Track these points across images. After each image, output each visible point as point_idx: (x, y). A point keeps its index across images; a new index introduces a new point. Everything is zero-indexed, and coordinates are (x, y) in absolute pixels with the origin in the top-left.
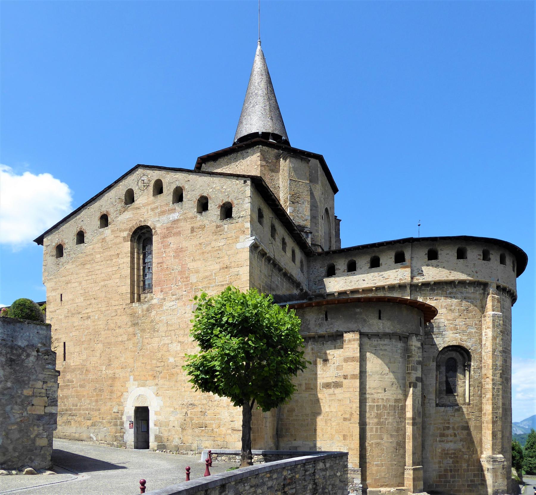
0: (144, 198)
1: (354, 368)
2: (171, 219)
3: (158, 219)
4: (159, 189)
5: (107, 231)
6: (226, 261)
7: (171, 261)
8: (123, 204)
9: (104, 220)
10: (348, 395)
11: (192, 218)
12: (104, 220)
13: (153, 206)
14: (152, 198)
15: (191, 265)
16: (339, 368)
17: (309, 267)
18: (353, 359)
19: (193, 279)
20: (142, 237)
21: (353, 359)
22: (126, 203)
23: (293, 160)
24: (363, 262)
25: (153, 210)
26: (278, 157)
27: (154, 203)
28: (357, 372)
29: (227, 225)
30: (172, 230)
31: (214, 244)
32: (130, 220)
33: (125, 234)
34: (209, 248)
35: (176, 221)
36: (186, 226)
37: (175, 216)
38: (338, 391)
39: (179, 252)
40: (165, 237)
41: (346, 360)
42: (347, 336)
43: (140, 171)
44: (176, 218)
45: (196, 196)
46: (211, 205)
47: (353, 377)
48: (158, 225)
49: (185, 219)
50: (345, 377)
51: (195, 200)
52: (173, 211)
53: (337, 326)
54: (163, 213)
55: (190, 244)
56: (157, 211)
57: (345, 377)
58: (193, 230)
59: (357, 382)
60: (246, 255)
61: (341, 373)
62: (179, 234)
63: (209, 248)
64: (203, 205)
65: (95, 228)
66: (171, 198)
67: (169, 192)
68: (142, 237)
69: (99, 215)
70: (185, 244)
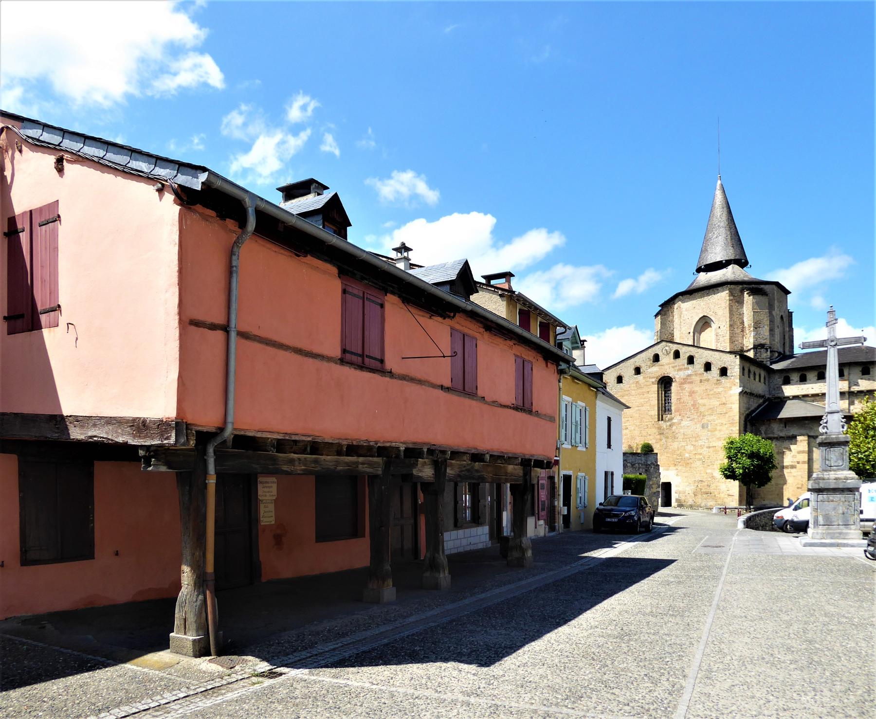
0: (666, 360)
1: (805, 457)
4: (677, 355)
5: (640, 377)
6: (724, 400)
7: (686, 398)
9: (638, 371)
10: (800, 473)
12: (638, 371)
15: (700, 401)
16: (794, 456)
17: (769, 378)
18: (803, 452)
19: (702, 409)
20: (665, 383)
21: (803, 452)
23: (756, 297)
24: (812, 375)
26: (742, 291)
28: (806, 459)
29: (723, 379)
30: (686, 380)
31: (715, 390)
32: (657, 372)
33: (654, 380)
34: (712, 392)
35: (689, 375)
36: (698, 378)
37: (689, 372)
38: (793, 470)
39: (692, 393)
40: (682, 384)
41: (799, 452)
42: (799, 438)
43: (664, 343)
47: (804, 462)
48: (677, 376)
49: (696, 375)
50: (798, 463)
53: (792, 431)
54: (680, 370)
55: (699, 389)
57: (798, 463)
58: (701, 381)
59: (806, 466)
60: (737, 397)
61: (796, 460)
62: (691, 383)
63: (712, 392)
64: (708, 367)
66: (686, 361)
68: (665, 383)
69: (633, 367)
70: (696, 389)
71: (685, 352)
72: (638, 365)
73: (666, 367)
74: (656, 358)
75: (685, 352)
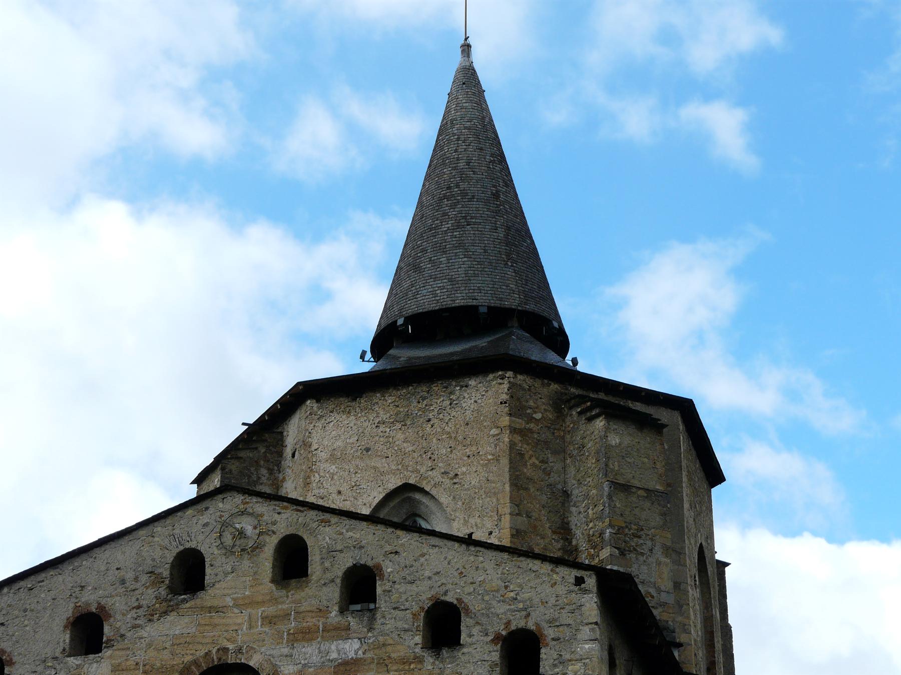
2: (334, 655)
3: (286, 651)
4: (292, 561)
8: (163, 591)
11: (404, 661)
13: (271, 610)
14: (267, 586)
22: (173, 590)
25: (269, 621)
27: (274, 601)
37: (351, 648)
44: (351, 655)
45: (423, 594)
46: (470, 632)
51: (416, 608)
52: (343, 632)
54: (305, 635)
56: (283, 627)
65: (48, 652)
66: (334, 593)
67: (329, 576)
71: (332, 551)
72: (90, 599)
73: (237, 618)
74: (189, 574)
75: (332, 551)
